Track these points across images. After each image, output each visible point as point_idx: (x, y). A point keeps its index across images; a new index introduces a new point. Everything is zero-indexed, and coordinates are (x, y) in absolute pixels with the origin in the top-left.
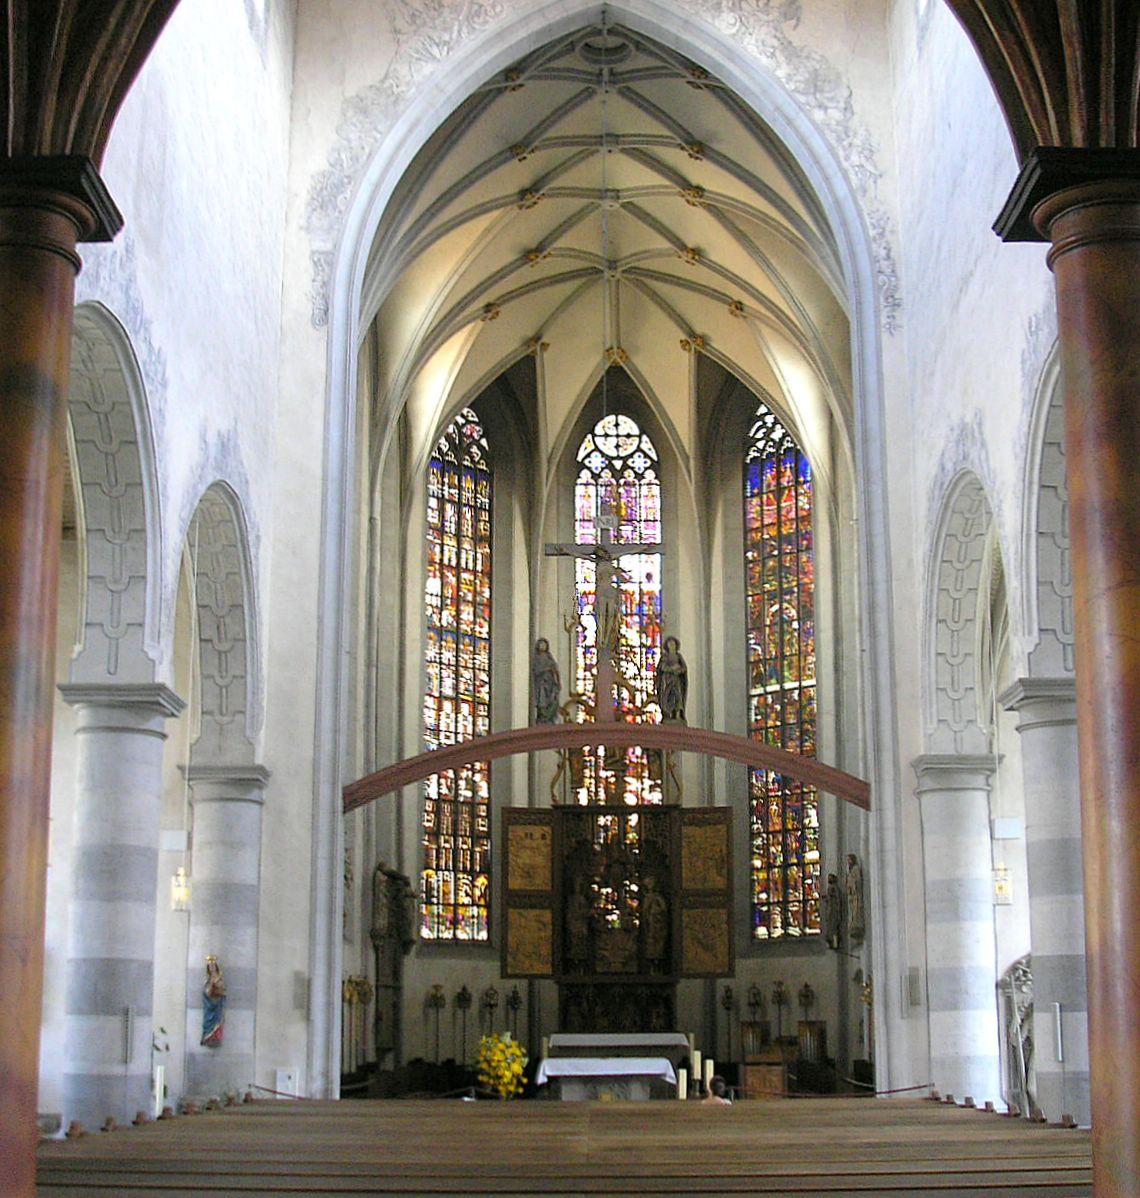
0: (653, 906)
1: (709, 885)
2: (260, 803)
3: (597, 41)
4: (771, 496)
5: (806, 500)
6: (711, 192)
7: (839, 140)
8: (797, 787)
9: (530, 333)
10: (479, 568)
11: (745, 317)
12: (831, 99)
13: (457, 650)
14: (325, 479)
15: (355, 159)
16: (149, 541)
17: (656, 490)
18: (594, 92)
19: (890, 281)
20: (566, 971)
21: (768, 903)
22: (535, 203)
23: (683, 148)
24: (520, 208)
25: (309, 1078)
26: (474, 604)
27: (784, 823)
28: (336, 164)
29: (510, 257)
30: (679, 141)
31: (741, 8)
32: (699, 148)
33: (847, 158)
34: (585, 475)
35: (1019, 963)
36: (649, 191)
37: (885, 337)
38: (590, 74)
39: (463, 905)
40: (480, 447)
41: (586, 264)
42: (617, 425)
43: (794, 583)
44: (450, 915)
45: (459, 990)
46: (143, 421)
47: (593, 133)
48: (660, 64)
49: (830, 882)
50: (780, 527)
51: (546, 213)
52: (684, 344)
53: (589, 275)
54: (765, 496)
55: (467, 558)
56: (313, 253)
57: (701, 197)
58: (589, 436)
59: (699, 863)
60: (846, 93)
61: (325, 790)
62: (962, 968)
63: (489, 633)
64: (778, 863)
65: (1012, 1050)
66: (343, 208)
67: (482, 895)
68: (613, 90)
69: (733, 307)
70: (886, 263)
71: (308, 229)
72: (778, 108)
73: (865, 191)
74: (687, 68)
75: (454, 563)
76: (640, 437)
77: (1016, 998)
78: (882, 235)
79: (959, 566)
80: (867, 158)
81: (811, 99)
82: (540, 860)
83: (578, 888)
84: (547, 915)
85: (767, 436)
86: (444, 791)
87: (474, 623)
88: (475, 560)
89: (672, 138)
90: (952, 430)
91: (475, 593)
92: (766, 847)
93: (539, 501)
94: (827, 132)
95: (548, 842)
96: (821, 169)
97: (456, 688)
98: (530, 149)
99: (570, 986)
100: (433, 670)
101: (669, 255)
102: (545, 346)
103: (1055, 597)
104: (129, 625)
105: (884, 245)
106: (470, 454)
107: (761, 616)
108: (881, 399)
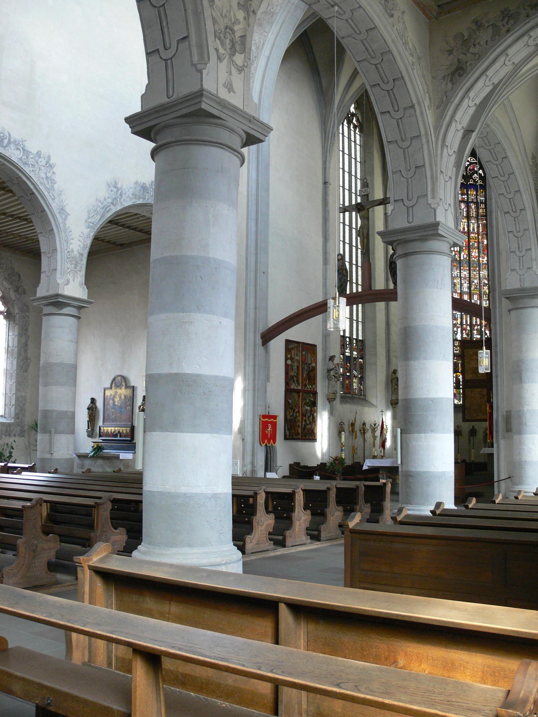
13: (469, 270)
16: (56, 234)
25: (243, 465)
61: (251, 336)
62: (523, 410)
63: (488, 261)
66: (253, 72)
79: (503, 179)
86: (465, 336)
87: (479, 256)
91: (479, 243)
97: (470, 288)
100: (457, 281)
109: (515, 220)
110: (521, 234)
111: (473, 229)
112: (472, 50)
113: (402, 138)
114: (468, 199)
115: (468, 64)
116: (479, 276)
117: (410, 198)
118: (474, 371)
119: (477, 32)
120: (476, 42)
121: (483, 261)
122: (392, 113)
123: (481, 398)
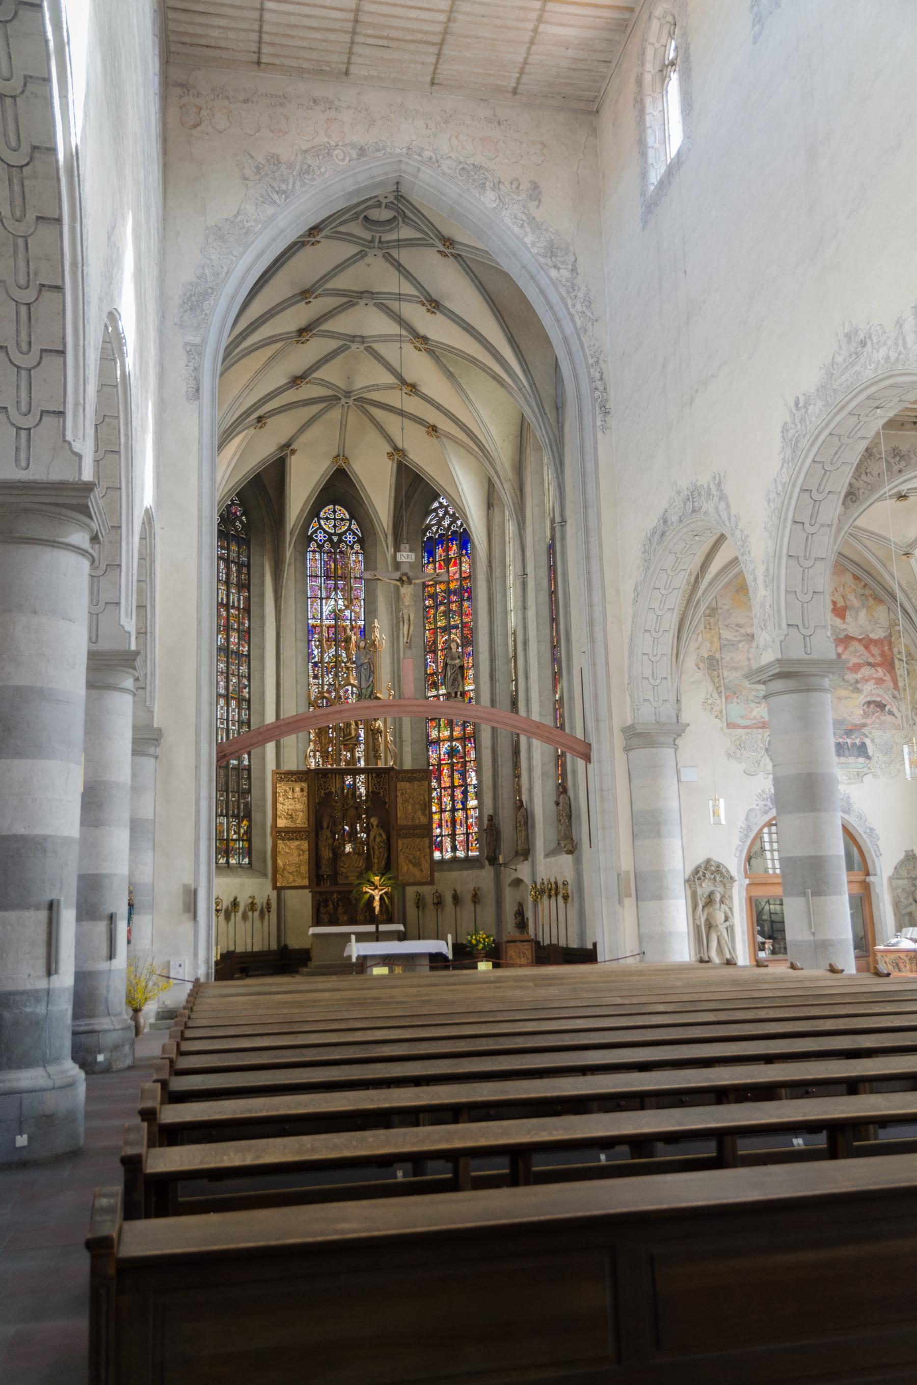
0: (377, 836)
1: (417, 822)
2: (156, 758)
3: (374, 214)
4: (442, 563)
5: (467, 566)
6: (434, 341)
7: (568, 292)
8: (461, 758)
9: (283, 441)
10: (242, 607)
11: (438, 437)
12: (562, 262)
13: (228, 662)
14: (200, 517)
15: (216, 275)
17: (361, 558)
18: (366, 255)
19: (603, 396)
20: (318, 884)
21: (441, 835)
22: (308, 340)
23: (423, 304)
24: (298, 342)
25: (196, 966)
26: (238, 630)
27: (453, 782)
28: (202, 277)
29: (283, 381)
30: (423, 299)
31: (499, 189)
32: (434, 305)
33: (574, 306)
34: (313, 546)
35: (699, 866)
36: (386, 339)
37: (600, 435)
38: (365, 240)
39: (232, 840)
40: (242, 522)
41: (329, 392)
42: (334, 512)
43: (459, 622)
44: (224, 846)
45: (232, 900)
46: (126, 436)
47: (356, 289)
48: (419, 235)
49: (489, 820)
50: (449, 583)
51: (316, 348)
52: (390, 455)
53: (332, 400)
54: (437, 565)
55: (234, 598)
56: (186, 344)
57: (426, 344)
58: (316, 519)
59: (410, 808)
60: (573, 259)
63: (249, 651)
64: (448, 808)
65: (697, 928)
66: (208, 312)
67: (246, 833)
68: (380, 253)
69: (431, 429)
70: (599, 382)
71: (181, 326)
72: (524, 267)
73: (586, 331)
74: (440, 240)
75: (225, 602)
76: (350, 520)
77: (699, 891)
78: (597, 362)
80: (588, 307)
81: (548, 260)
82: (299, 806)
83: (325, 825)
84: (305, 845)
85: (439, 523)
87: (239, 644)
88: (239, 600)
89: (419, 298)
90: (679, 493)
92: (440, 799)
93: (283, 562)
94: (560, 286)
95: (305, 794)
96: (554, 314)
97: (227, 688)
98: (314, 295)
99: (321, 893)
101: (392, 388)
102: (293, 452)
103: (797, 601)
104: (106, 603)
105: (598, 370)
106: (235, 526)
107: (435, 642)
108: (597, 478)
109: (654, 642)
110: (657, 658)
111: (233, 602)
112: (863, 477)
113: (805, 556)
114: (228, 556)
115: (861, 491)
116: (239, 672)
117: (806, 625)
118: (291, 815)
119: (869, 461)
120: (868, 471)
121: (243, 651)
122: (807, 525)
123: (300, 855)
